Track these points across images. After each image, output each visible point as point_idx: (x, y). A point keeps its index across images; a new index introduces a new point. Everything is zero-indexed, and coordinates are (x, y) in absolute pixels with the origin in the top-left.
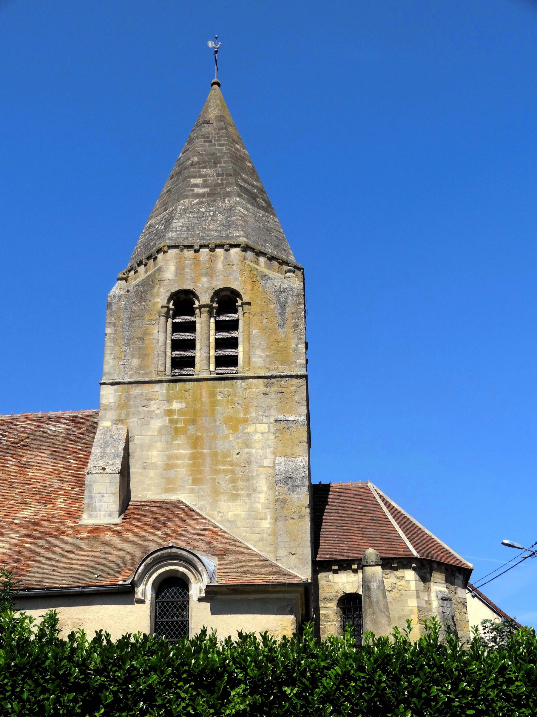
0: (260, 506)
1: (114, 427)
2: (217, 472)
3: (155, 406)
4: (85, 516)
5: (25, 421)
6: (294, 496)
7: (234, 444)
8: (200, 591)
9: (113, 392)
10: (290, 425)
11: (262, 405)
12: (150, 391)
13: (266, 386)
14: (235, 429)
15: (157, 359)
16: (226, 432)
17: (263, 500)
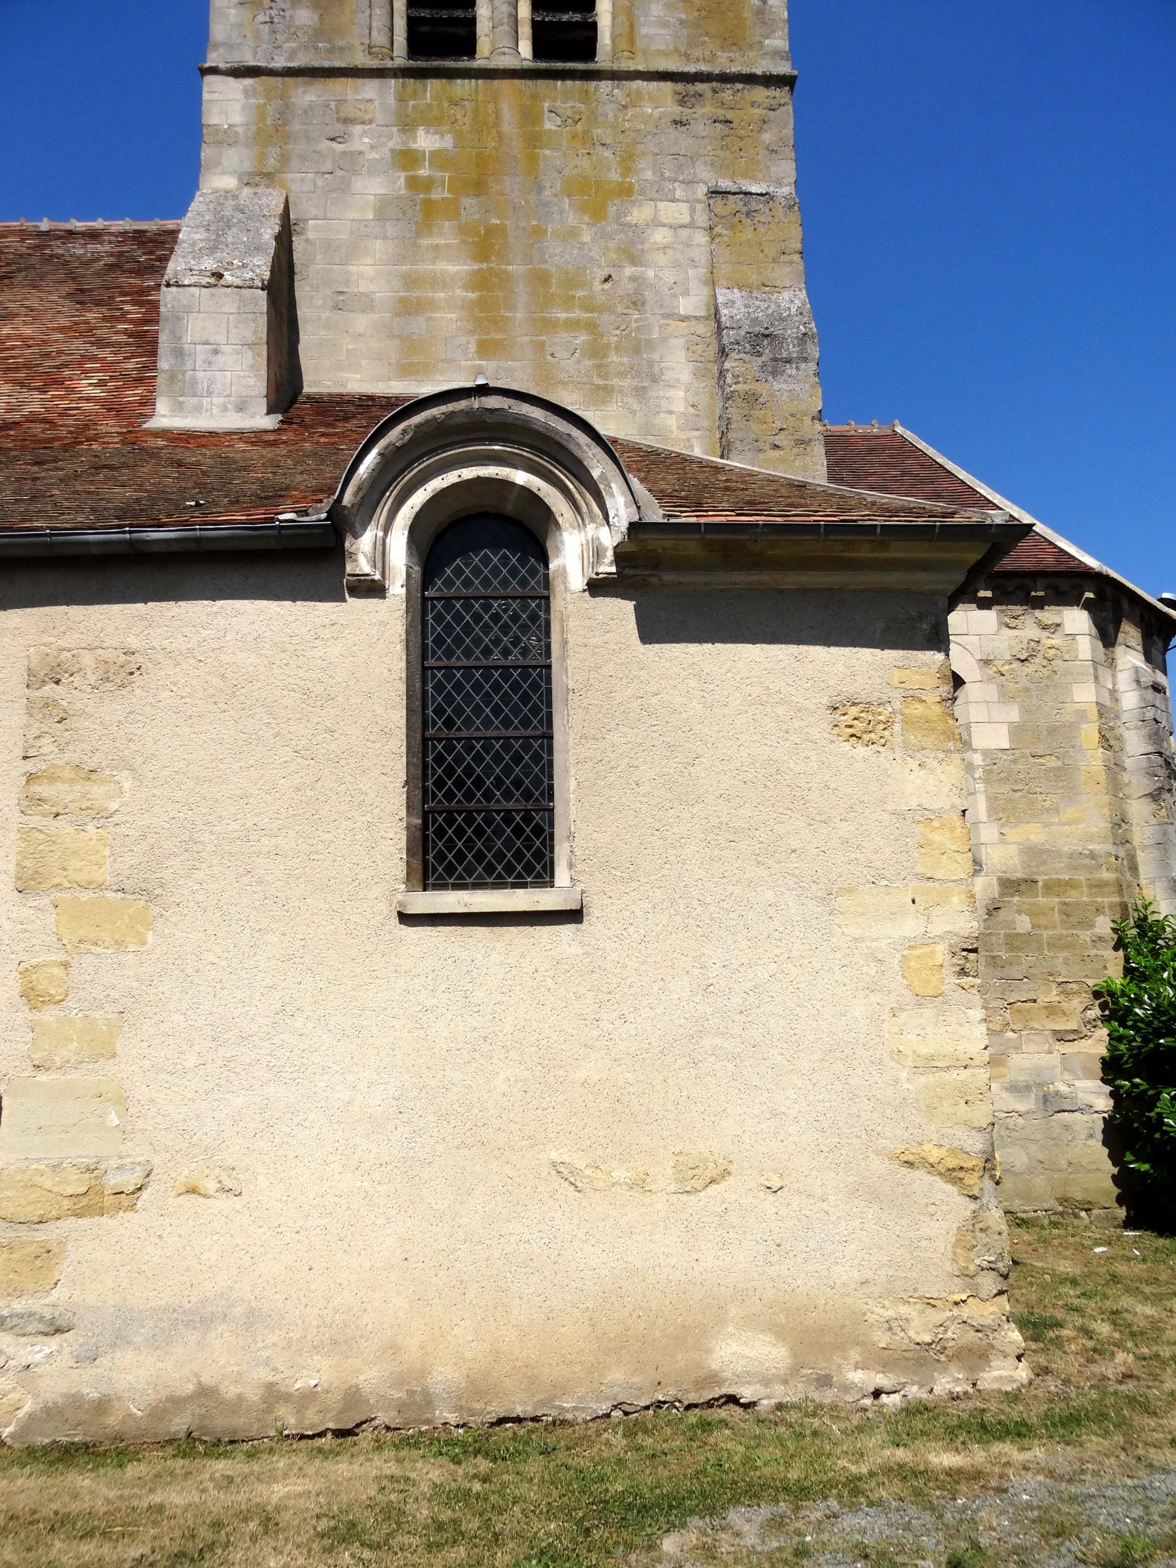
0: (672, 422)
1: (246, 191)
2: (549, 325)
3: (366, 140)
4: (162, 406)
6: (778, 385)
7: (594, 254)
8: (598, 553)
9: (240, 96)
10: (754, 205)
11: (673, 151)
12: (349, 97)
13: (682, 102)
14: (597, 213)
15: (367, 13)
16: (572, 219)
17: (680, 406)
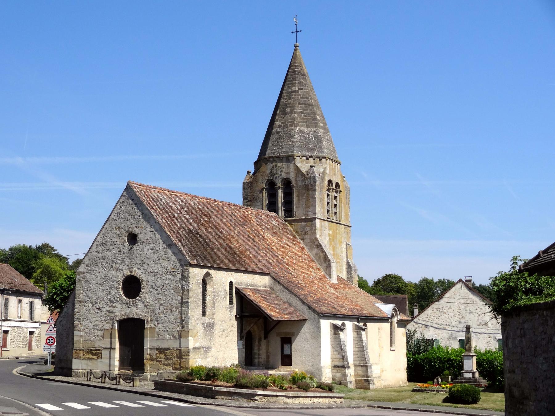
5: (262, 215)
